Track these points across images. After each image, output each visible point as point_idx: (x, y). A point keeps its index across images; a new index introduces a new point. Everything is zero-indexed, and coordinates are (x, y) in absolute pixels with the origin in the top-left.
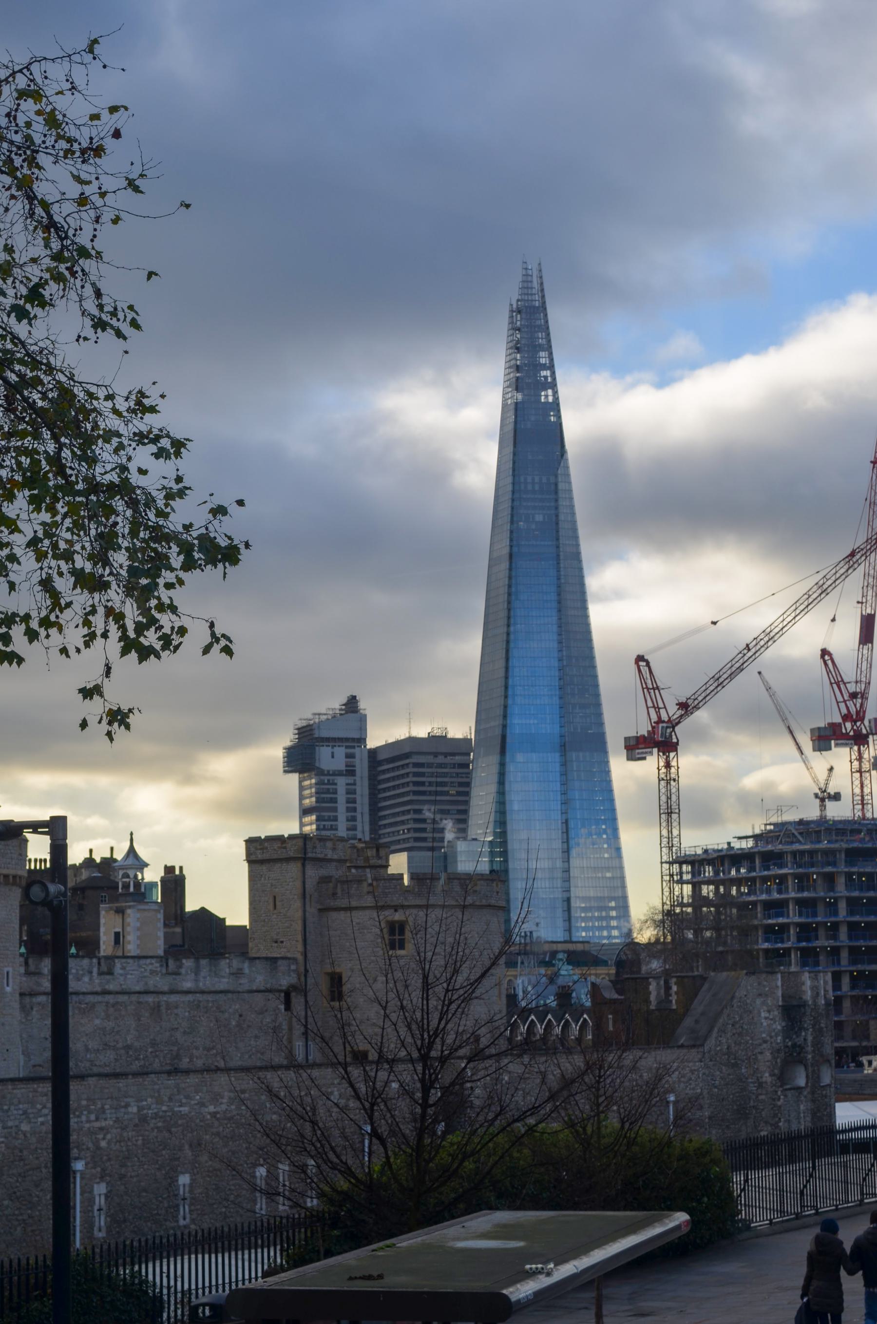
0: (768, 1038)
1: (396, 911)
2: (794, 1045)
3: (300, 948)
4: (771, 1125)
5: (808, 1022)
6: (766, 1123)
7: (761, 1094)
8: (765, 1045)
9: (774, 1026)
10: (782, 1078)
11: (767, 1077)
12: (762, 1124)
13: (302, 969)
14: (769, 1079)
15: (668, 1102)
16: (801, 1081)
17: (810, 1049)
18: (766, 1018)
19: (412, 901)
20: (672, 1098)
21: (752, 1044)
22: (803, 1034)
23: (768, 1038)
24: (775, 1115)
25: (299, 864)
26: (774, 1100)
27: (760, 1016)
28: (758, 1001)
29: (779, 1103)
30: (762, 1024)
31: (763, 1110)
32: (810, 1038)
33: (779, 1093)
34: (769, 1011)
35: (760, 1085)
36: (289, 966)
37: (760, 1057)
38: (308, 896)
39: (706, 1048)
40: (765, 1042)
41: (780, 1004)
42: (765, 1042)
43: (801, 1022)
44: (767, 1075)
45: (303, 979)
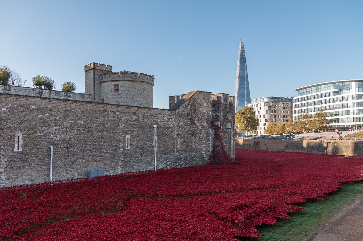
1: (116, 82)
2: (216, 115)
3: (93, 92)
4: (206, 139)
5: (221, 108)
6: (205, 138)
7: (203, 129)
9: (209, 109)
11: (205, 124)
12: (203, 138)
13: (93, 98)
15: (154, 128)
17: (222, 117)
18: (206, 106)
19: (120, 79)
20: (155, 126)
21: (200, 114)
22: (220, 112)
23: (206, 112)
24: (208, 136)
26: (208, 131)
27: (204, 105)
28: (203, 101)
29: (210, 132)
30: (204, 108)
31: (203, 134)
32: (222, 114)
33: (210, 129)
34: (207, 104)
35: (203, 126)
36: (89, 96)
37: (203, 118)
38: (96, 80)
39: (176, 111)
40: (205, 113)
41: (211, 102)
42: (205, 113)
43: (219, 108)
44: (205, 123)
45: (93, 100)
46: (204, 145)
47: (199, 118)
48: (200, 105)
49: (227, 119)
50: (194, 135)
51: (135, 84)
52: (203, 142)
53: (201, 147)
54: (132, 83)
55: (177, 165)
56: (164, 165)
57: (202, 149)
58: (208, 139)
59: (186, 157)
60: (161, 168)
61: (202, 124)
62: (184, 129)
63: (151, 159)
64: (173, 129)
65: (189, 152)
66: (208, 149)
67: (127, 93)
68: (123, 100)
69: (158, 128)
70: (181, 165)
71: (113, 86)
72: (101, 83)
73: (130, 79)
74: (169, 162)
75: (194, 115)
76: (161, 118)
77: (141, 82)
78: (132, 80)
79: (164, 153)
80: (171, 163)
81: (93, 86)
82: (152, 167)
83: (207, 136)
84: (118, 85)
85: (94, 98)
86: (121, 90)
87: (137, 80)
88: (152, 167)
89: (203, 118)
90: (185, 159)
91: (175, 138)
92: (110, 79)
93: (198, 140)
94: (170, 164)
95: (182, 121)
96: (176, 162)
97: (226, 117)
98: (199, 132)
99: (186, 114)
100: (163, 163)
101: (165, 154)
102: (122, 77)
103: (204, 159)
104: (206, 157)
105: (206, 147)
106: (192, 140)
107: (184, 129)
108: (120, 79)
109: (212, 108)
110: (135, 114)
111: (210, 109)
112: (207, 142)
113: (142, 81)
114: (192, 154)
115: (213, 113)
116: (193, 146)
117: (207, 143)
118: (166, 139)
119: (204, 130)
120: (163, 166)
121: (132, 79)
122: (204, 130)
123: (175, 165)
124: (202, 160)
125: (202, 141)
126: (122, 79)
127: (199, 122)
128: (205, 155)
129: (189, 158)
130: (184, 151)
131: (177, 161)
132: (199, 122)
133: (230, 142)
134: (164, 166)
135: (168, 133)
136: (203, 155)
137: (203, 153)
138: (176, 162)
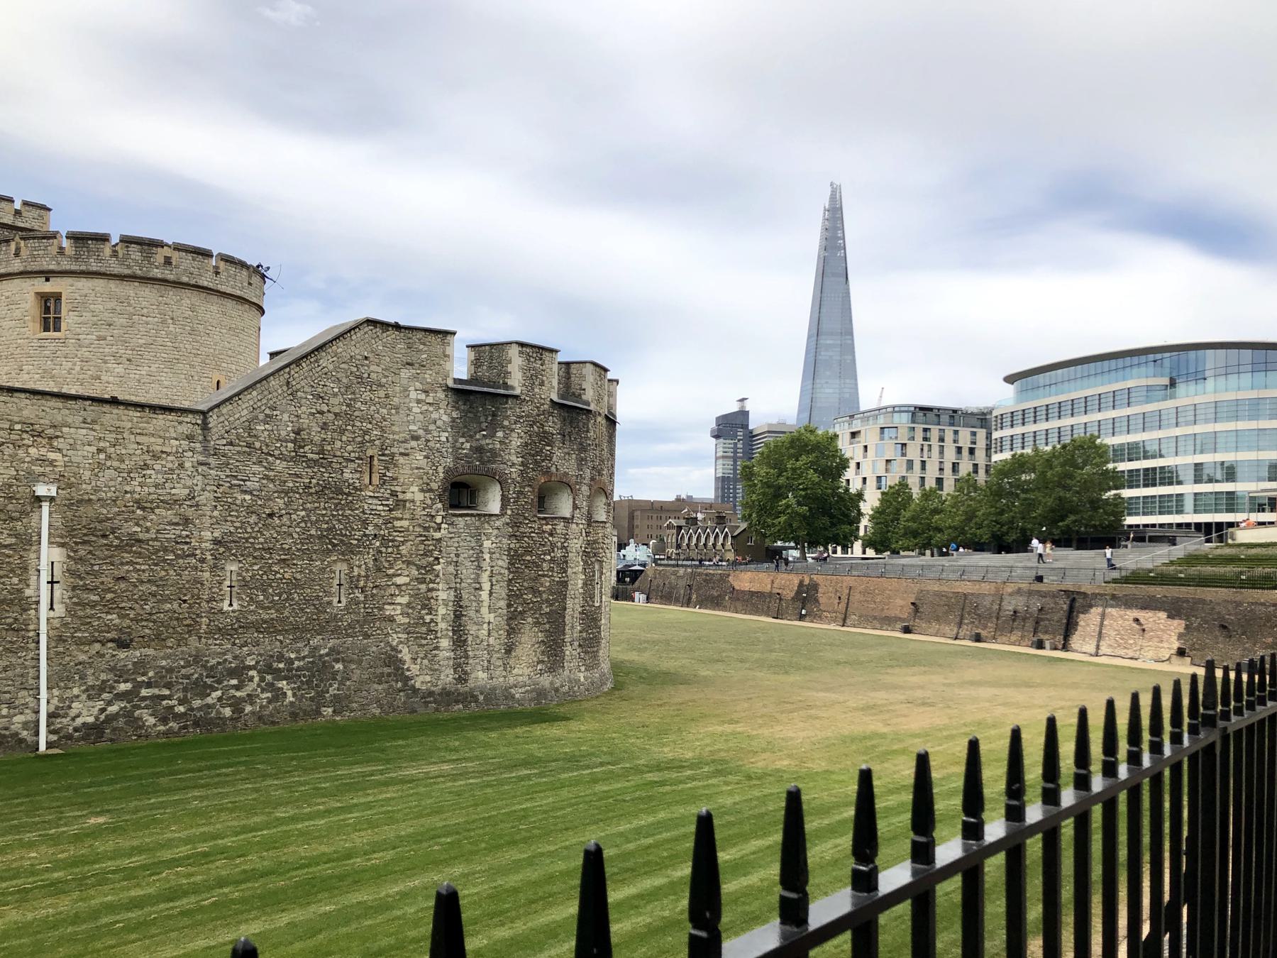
0: (421, 432)
1: (47, 280)
2: (479, 450)
4: (419, 568)
6: (409, 563)
7: (401, 519)
8: (414, 444)
11: (414, 493)
12: (399, 565)
14: (419, 497)
18: (419, 402)
19: (66, 265)
22: (500, 434)
23: (421, 432)
26: (427, 529)
28: (405, 373)
29: (437, 535)
30: (410, 409)
31: (403, 543)
32: (516, 442)
33: (439, 520)
35: (401, 504)
40: (416, 438)
43: (494, 415)
46: (404, 600)
47: (376, 462)
48: (382, 394)
49: (547, 472)
50: (334, 545)
51: (146, 296)
52: (400, 580)
53: (381, 609)
54: (129, 289)
55: (209, 700)
56: (109, 703)
57: (391, 619)
58: (429, 569)
59: (281, 658)
60: (91, 720)
61: (394, 494)
62: (271, 515)
63: (10, 673)
64: (190, 513)
65: (300, 631)
66: (428, 618)
67: (100, 338)
68: (77, 368)
69: (70, 505)
70: (237, 705)
71: (30, 305)
73: (116, 269)
74: (149, 685)
75: (338, 444)
76: (94, 449)
77: (178, 284)
78: (127, 272)
79: (112, 641)
80: (167, 692)
82: (19, 719)
83: (425, 555)
84: (57, 297)
86: (69, 319)
87: (157, 273)
88: (19, 719)
89: (401, 460)
90: (269, 669)
91: (203, 561)
92: (17, 266)
93: (367, 569)
94: (165, 697)
95: (256, 468)
96: (206, 686)
97: (536, 462)
98: (371, 530)
99: (283, 433)
100: (105, 696)
101: (123, 644)
102: (76, 258)
103: (397, 669)
104: (414, 660)
105: (413, 608)
106: (323, 570)
107: (271, 515)
108: (68, 267)
109: (455, 415)
111: (445, 418)
112: (423, 581)
113: (185, 279)
114: (324, 644)
115: (462, 440)
116: (330, 603)
117: (423, 587)
118: (131, 563)
119: (405, 523)
120: (103, 710)
121: (129, 267)
122: (405, 523)
123: (197, 703)
124: (389, 675)
125: (391, 576)
126: (73, 268)
127: (376, 480)
128: (405, 650)
129: (297, 663)
130: (269, 628)
131: (209, 681)
132: (376, 480)
133: (564, 584)
134: (113, 709)
135: (148, 530)
136: (393, 649)
137: (394, 640)
138: (204, 691)
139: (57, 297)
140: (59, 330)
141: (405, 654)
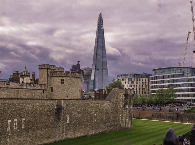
3: (46, 83)
10: (124, 106)
11: (121, 106)
13: (46, 86)
16: (127, 107)
19: (65, 76)
25: (47, 69)
28: (121, 94)
51: (73, 79)
71: (60, 80)
72: (51, 77)
81: (46, 79)
84: (63, 80)
85: (47, 87)
92: (58, 75)
110: (98, 103)
139: (63, 80)
140: (63, 83)
141: (121, 124)
